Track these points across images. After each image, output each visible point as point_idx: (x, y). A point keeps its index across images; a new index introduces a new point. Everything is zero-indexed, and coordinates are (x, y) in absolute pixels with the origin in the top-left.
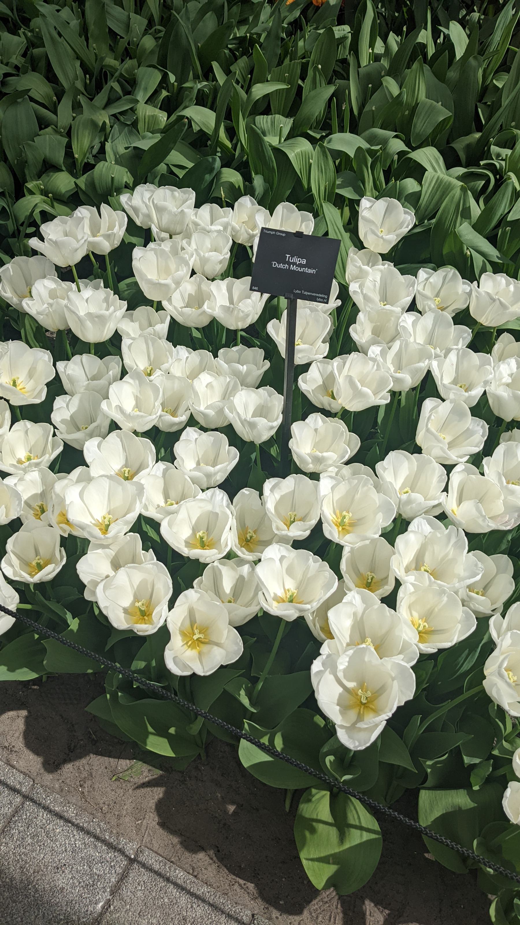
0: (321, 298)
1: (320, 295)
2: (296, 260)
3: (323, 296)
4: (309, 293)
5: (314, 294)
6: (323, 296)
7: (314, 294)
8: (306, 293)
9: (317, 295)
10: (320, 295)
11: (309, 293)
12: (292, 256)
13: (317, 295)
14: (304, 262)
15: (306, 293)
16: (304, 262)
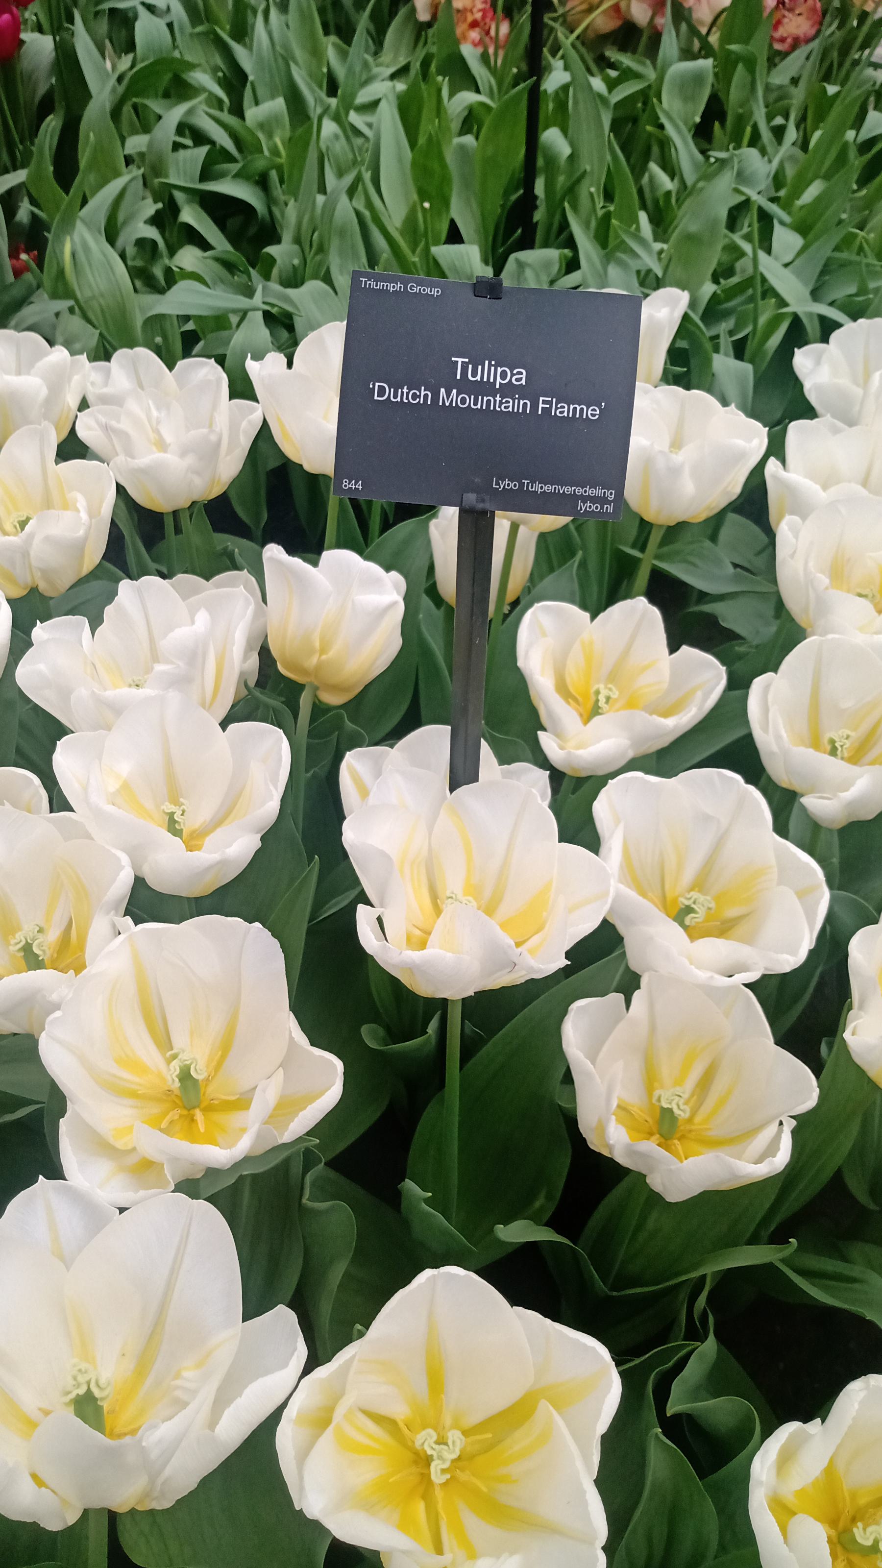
0: (594, 500)
1: (590, 492)
2: (488, 372)
3: (598, 492)
4: (548, 488)
5: (568, 490)
6: (598, 492)
7: (568, 490)
8: (537, 487)
9: (579, 491)
10: (590, 492)
11: (548, 488)
12: (476, 362)
13: (579, 491)
14: (521, 377)
15: (537, 487)
16: (521, 377)
